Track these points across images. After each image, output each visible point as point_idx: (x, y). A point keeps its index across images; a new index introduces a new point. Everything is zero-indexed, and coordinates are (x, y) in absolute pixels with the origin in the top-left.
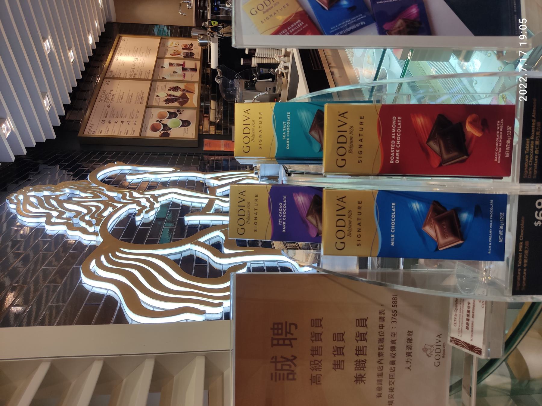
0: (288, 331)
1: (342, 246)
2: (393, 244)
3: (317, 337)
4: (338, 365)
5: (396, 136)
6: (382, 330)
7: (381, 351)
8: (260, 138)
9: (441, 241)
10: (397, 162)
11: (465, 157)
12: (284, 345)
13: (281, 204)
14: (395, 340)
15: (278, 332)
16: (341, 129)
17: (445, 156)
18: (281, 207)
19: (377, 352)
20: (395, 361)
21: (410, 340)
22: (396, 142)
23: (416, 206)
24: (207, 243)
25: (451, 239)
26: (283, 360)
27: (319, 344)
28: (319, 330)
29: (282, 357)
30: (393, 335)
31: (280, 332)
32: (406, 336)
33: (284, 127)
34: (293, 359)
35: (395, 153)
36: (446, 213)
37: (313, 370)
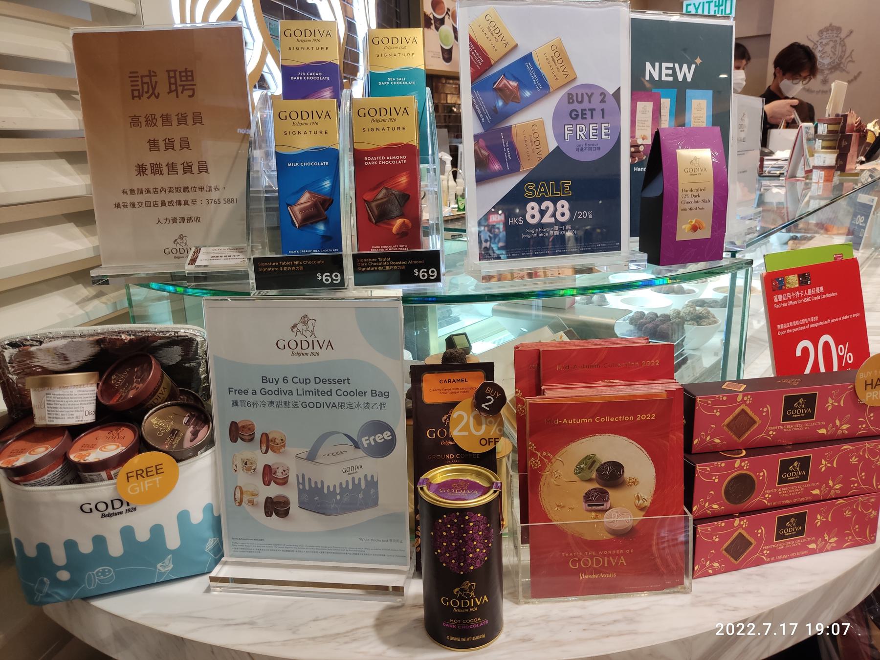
0: (186, 87)
1: (283, 117)
2: (289, 165)
3: (182, 119)
4: (153, 144)
5: (389, 160)
6: (197, 190)
7: (175, 190)
8: (388, 55)
9: (297, 209)
10: (366, 163)
11: (374, 221)
12: (170, 84)
13: (320, 74)
14: (188, 205)
15: (183, 76)
16: (393, 111)
17: (373, 204)
18: (317, 74)
19: (173, 186)
20: (165, 206)
21: (190, 220)
22: (383, 160)
23: (327, 184)
24: (265, 69)
25: (300, 217)
26: (154, 84)
27: (175, 123)
28: (190, 121)
29: (156, 82)
30: (194, 202)
31: (184, 79)
32: (194, 216)
33: (400, 79)
34: (155, 96)
35: (374, 161)
36: (323, 211)
37: (145, 117)
